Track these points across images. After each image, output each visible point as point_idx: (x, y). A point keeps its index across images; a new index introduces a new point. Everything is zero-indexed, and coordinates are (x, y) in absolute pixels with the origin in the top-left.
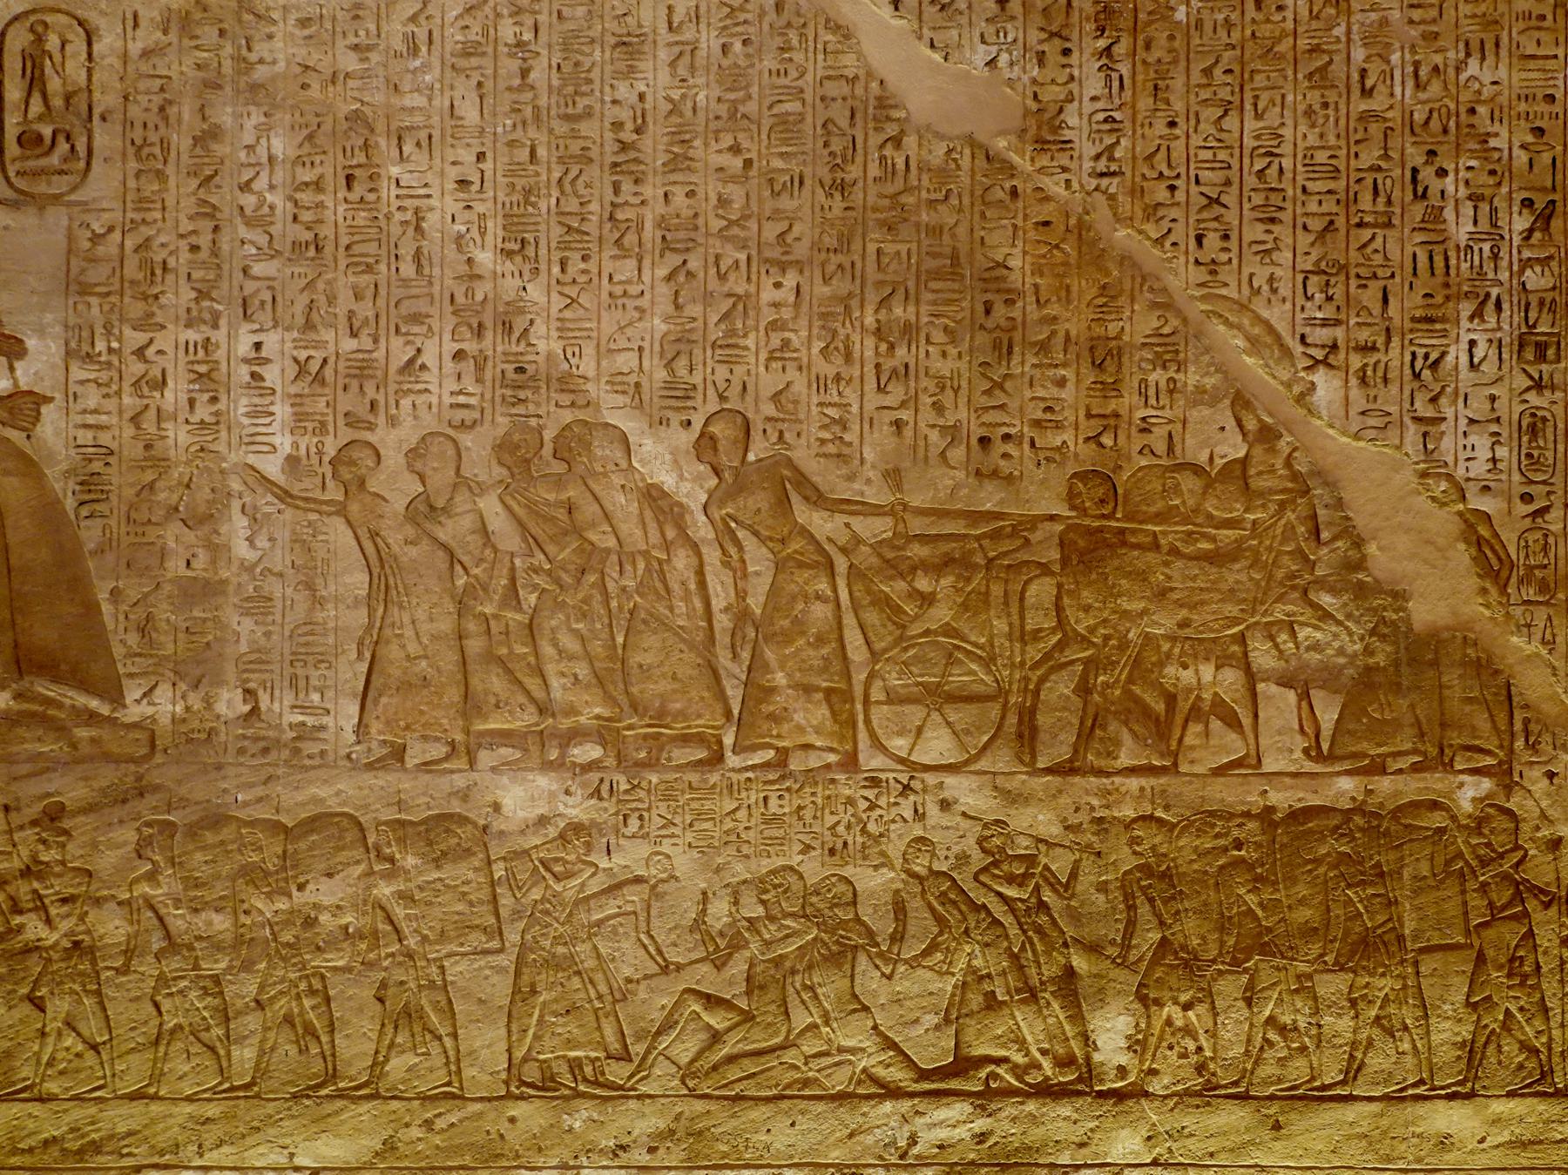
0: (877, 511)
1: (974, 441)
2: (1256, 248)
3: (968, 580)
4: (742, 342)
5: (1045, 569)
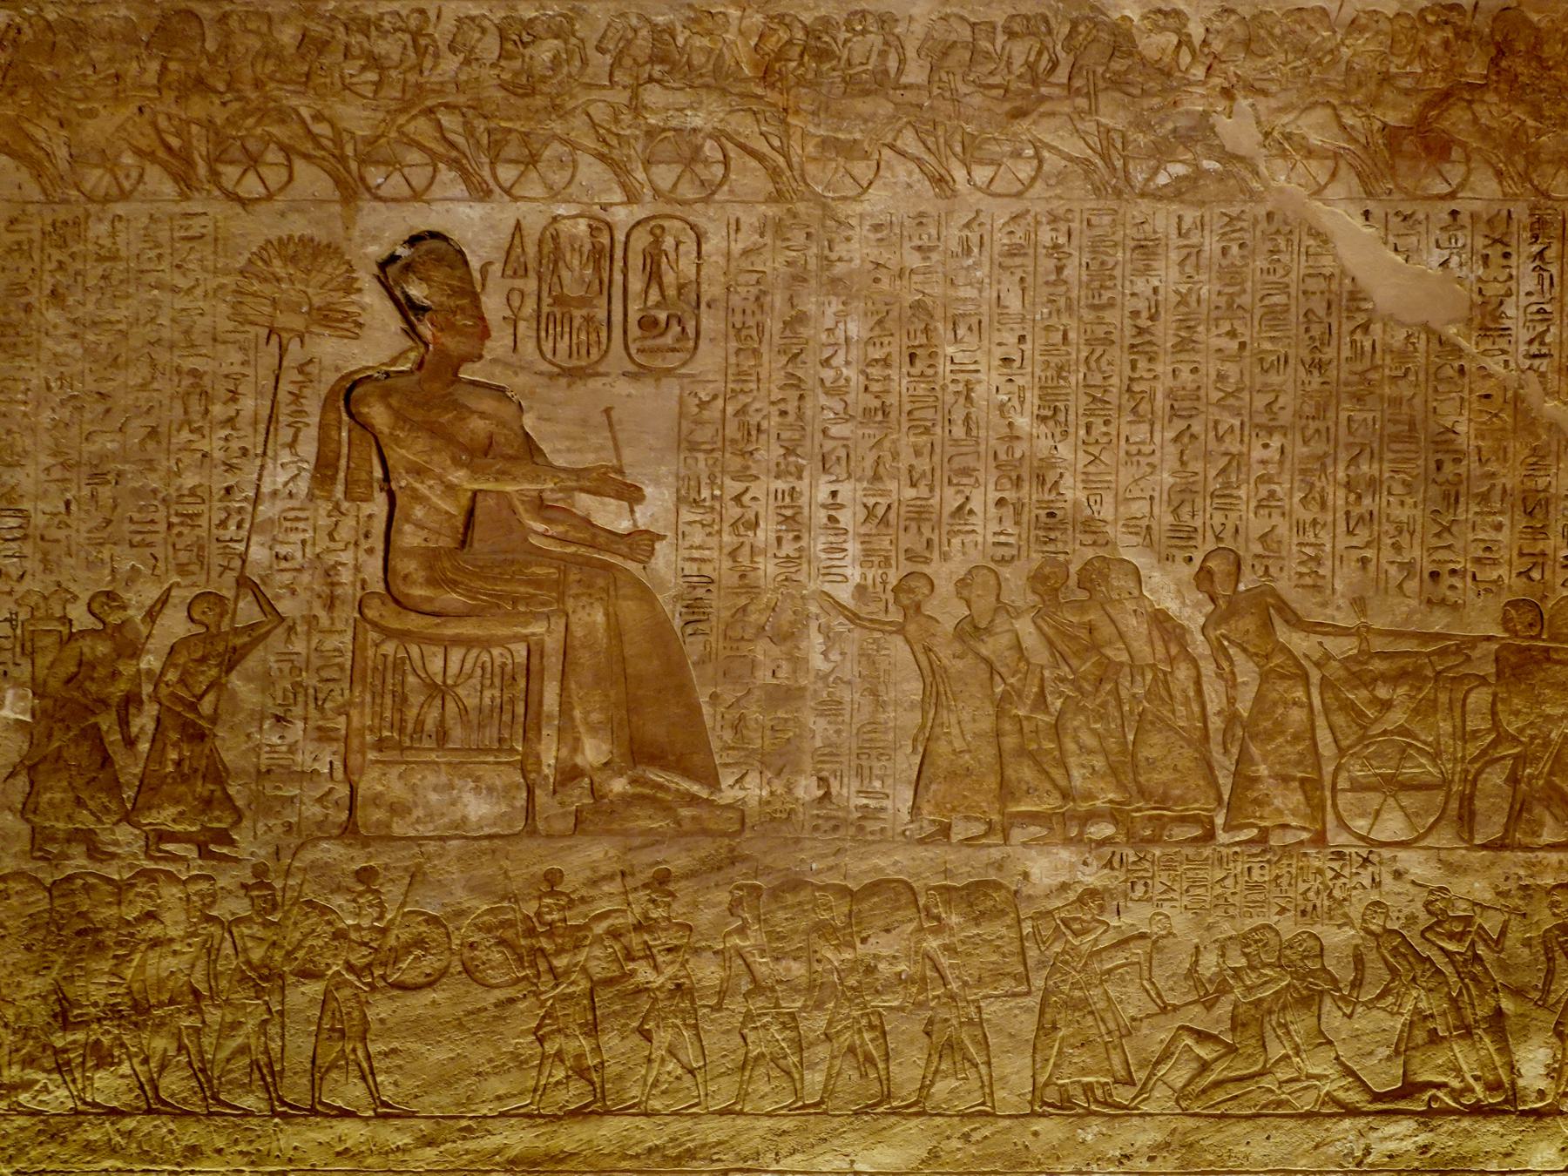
1: (1426, 575)
3: (1420, 689)
5: (1483, 681)
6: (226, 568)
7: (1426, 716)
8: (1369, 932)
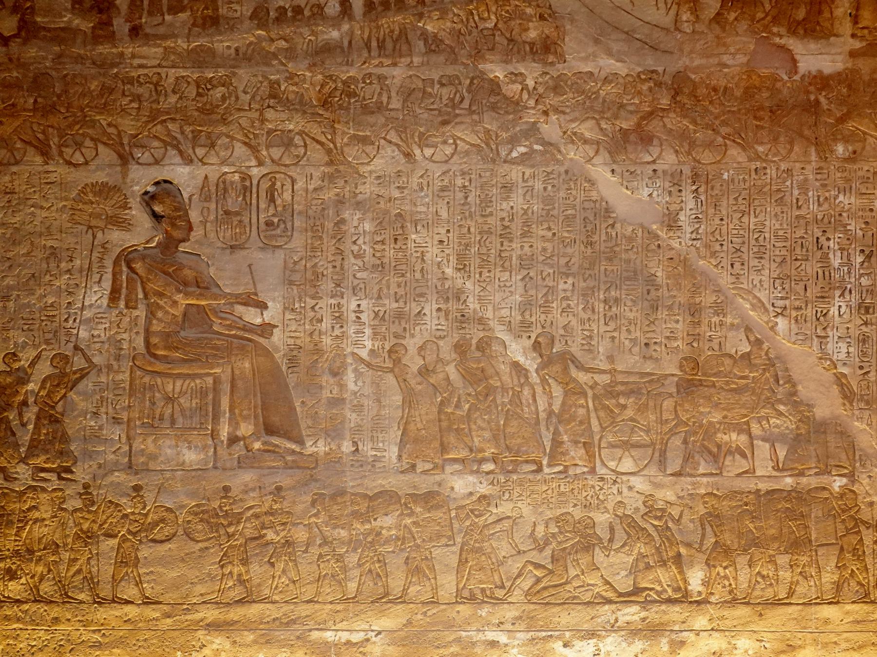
0: (603, 372)
1: (643, 344)
2: (755, 269)
3: (640, 399)
4: (551, 305)
5: (671, 395)
6: (68, 341)
7: (643, 413)
8: (616, 515)
